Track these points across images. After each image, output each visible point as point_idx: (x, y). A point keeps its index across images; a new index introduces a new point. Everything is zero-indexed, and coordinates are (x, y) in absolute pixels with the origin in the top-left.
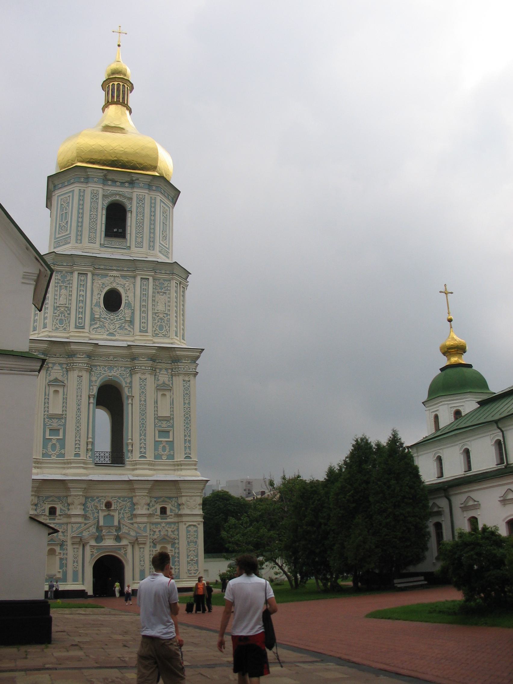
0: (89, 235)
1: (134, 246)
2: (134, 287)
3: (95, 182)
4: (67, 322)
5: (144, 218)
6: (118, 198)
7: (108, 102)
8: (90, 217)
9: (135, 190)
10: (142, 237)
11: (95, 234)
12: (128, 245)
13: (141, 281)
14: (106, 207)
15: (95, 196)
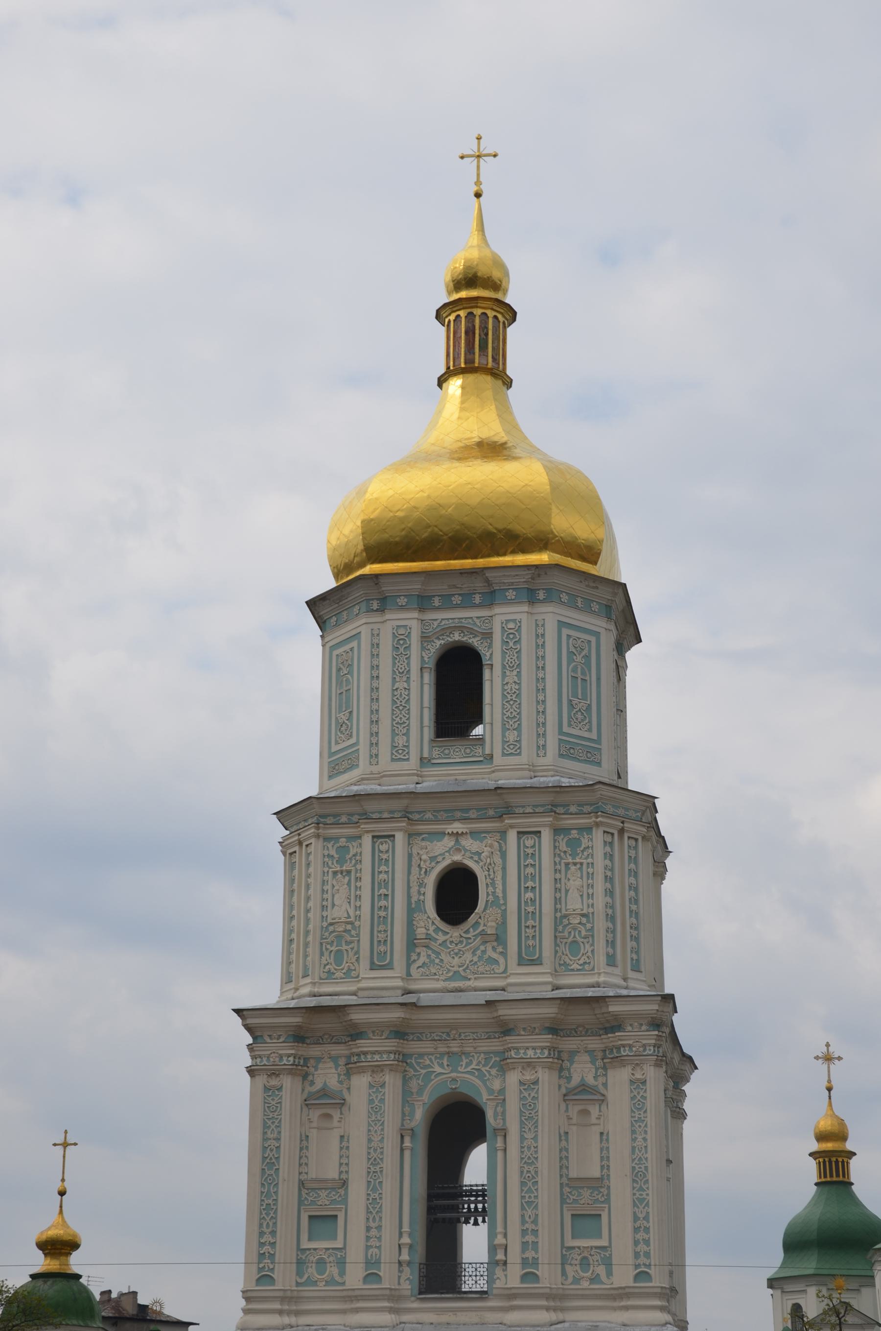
0: (393, 741)
1: (500, 752)
2: (504, 855)
3: (402, 608)
4: (351, 954)
5: (519, 678)
6: (457, 637)
7: (448, 368)
8: (394, 695)
9: (497, 610)
10: (518, 729)
11: (405, 737)
12: (487, 751)
13: (519, 839)
14: (431, 664)
15: (401, 642)
